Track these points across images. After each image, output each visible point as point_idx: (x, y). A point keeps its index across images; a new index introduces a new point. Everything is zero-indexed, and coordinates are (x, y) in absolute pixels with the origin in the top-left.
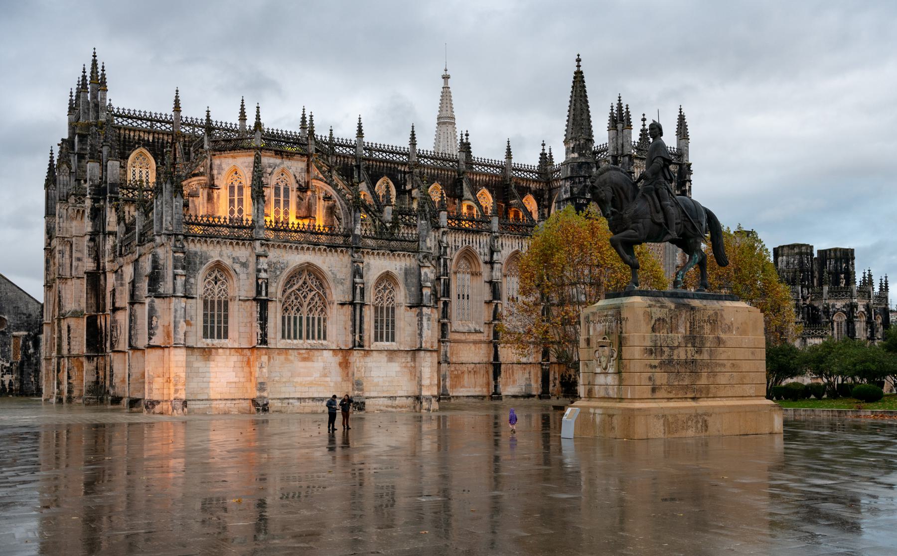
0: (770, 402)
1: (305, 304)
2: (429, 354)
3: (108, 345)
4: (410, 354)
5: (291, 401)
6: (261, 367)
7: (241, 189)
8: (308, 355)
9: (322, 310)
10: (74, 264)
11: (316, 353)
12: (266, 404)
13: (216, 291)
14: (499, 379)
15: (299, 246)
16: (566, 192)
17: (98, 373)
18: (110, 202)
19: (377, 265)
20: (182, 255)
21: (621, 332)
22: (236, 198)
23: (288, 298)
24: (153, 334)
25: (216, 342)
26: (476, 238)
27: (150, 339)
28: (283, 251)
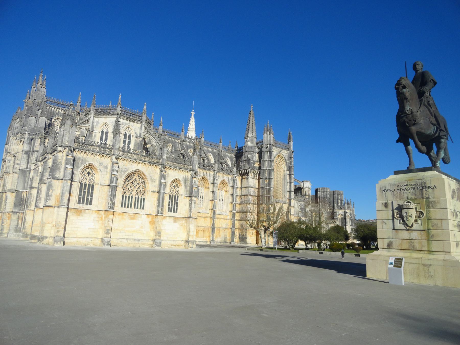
1: (135, 190)
2: (194, 219)
5: (123, 240)
6: (109, 221)
7: (107, 133)
8: (134, 217)
9: (143, 195)
10: (16, 166)
12: (109, 241)
13: (88, 179)
14: (215, 235)
15: (135, 161)
16: (245, 157)
17: (18, 221)
18: (38, 136)
19: (173, 174)
20: (71, 158)
21: (429, 198)
22: (104, 137)
24: (49, 199)
25: (85, 206)
26: (208, 172)
27: (47, 201)
28: (127, 162)
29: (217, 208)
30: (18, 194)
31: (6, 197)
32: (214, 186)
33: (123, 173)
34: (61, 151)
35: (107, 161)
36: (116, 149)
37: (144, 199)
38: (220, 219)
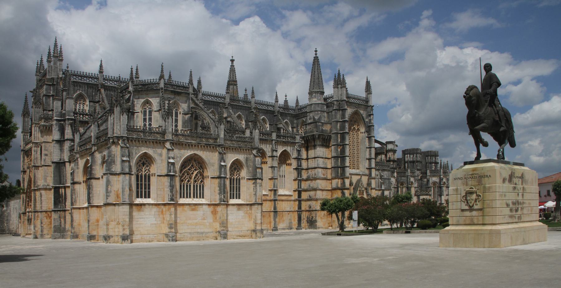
3: (68, 203)
7: (150, 112)
9: (202, 181)
11: (199, 206)
13: (143, 170)
22: (148, 117)
23: (183, 174)
27: (107, 198)
29: (278, 187)
31: (41, 194)
32: (273, 160)
36: (169, 133)
37: (203, 186)
38: (282, 201)
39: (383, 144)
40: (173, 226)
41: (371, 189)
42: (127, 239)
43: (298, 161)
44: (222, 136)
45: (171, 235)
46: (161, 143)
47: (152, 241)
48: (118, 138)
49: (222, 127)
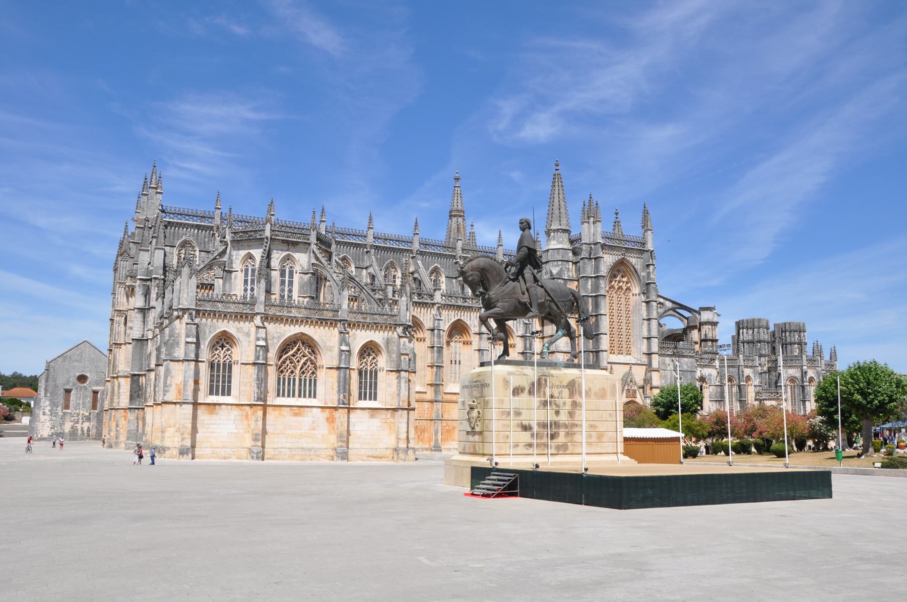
0: (627, 458)
1: (299, 368)
4: (390, 411)
9: (313, 373)
10: (128, 332)
15: (294, 321)
16: (546, 273)
22: (249, 278)
23: (284, 362)
24: (167, 391)
27: (165, 395)
30: (135, 378)
31: (119, 384)
32: (480, 338)
33: (275, 341)
34: (178, 317)
35: (248, 327)
36: (261, 303)
37: (315, 381)
39: (695, 311)
40: (260, 437)
41: (651, 388)
42: (187, 454)
43: (525, 340)
44: (345, 306)
45: (255, 451)
46: (249, 317)
47: (229, 458)
48: (184, 310)
49: (346, 293)
